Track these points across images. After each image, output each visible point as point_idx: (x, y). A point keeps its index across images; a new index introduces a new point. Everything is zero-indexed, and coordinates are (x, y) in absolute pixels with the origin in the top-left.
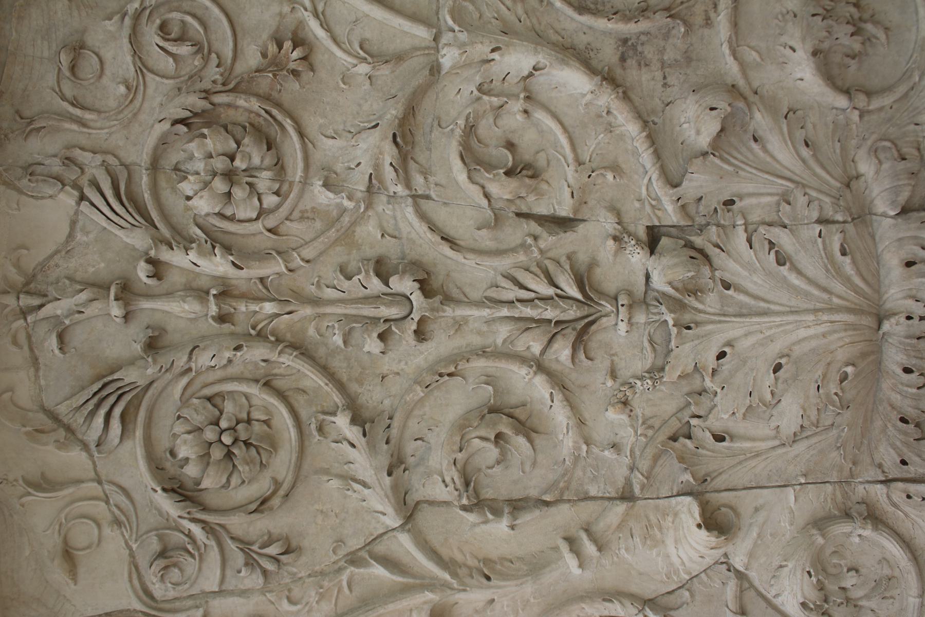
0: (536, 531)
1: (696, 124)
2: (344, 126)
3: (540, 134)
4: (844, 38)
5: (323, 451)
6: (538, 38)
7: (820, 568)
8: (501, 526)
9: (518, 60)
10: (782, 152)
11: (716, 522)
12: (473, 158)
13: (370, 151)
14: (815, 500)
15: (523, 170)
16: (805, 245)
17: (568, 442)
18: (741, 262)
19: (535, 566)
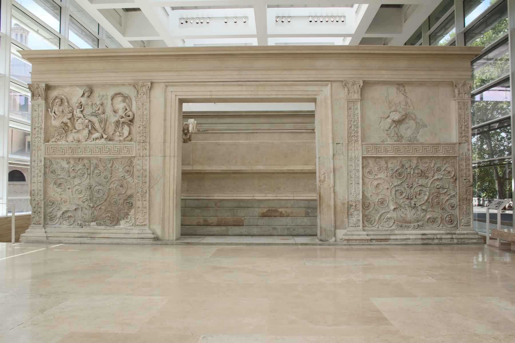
0: (394, 196)
1: (424, 207)
2: (422, 181)
3: (422, 196)
4: (432, 220)
5: (399, 180)
6: (429, 195)
7: (390, 218)
8: (394, 193)
9: (428, 194)
10: (422, 215)
11: (395, 209)
12: (420, 190)
13: (420, 183)
14: (395, 218)
15: (420, 194)
16: (415, 216)
17: (400, 198)
18: (414, 211)
19: (391, 195)
